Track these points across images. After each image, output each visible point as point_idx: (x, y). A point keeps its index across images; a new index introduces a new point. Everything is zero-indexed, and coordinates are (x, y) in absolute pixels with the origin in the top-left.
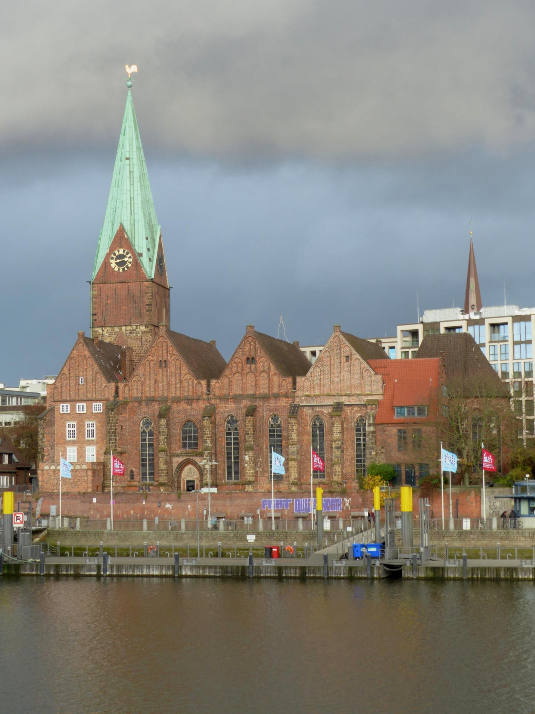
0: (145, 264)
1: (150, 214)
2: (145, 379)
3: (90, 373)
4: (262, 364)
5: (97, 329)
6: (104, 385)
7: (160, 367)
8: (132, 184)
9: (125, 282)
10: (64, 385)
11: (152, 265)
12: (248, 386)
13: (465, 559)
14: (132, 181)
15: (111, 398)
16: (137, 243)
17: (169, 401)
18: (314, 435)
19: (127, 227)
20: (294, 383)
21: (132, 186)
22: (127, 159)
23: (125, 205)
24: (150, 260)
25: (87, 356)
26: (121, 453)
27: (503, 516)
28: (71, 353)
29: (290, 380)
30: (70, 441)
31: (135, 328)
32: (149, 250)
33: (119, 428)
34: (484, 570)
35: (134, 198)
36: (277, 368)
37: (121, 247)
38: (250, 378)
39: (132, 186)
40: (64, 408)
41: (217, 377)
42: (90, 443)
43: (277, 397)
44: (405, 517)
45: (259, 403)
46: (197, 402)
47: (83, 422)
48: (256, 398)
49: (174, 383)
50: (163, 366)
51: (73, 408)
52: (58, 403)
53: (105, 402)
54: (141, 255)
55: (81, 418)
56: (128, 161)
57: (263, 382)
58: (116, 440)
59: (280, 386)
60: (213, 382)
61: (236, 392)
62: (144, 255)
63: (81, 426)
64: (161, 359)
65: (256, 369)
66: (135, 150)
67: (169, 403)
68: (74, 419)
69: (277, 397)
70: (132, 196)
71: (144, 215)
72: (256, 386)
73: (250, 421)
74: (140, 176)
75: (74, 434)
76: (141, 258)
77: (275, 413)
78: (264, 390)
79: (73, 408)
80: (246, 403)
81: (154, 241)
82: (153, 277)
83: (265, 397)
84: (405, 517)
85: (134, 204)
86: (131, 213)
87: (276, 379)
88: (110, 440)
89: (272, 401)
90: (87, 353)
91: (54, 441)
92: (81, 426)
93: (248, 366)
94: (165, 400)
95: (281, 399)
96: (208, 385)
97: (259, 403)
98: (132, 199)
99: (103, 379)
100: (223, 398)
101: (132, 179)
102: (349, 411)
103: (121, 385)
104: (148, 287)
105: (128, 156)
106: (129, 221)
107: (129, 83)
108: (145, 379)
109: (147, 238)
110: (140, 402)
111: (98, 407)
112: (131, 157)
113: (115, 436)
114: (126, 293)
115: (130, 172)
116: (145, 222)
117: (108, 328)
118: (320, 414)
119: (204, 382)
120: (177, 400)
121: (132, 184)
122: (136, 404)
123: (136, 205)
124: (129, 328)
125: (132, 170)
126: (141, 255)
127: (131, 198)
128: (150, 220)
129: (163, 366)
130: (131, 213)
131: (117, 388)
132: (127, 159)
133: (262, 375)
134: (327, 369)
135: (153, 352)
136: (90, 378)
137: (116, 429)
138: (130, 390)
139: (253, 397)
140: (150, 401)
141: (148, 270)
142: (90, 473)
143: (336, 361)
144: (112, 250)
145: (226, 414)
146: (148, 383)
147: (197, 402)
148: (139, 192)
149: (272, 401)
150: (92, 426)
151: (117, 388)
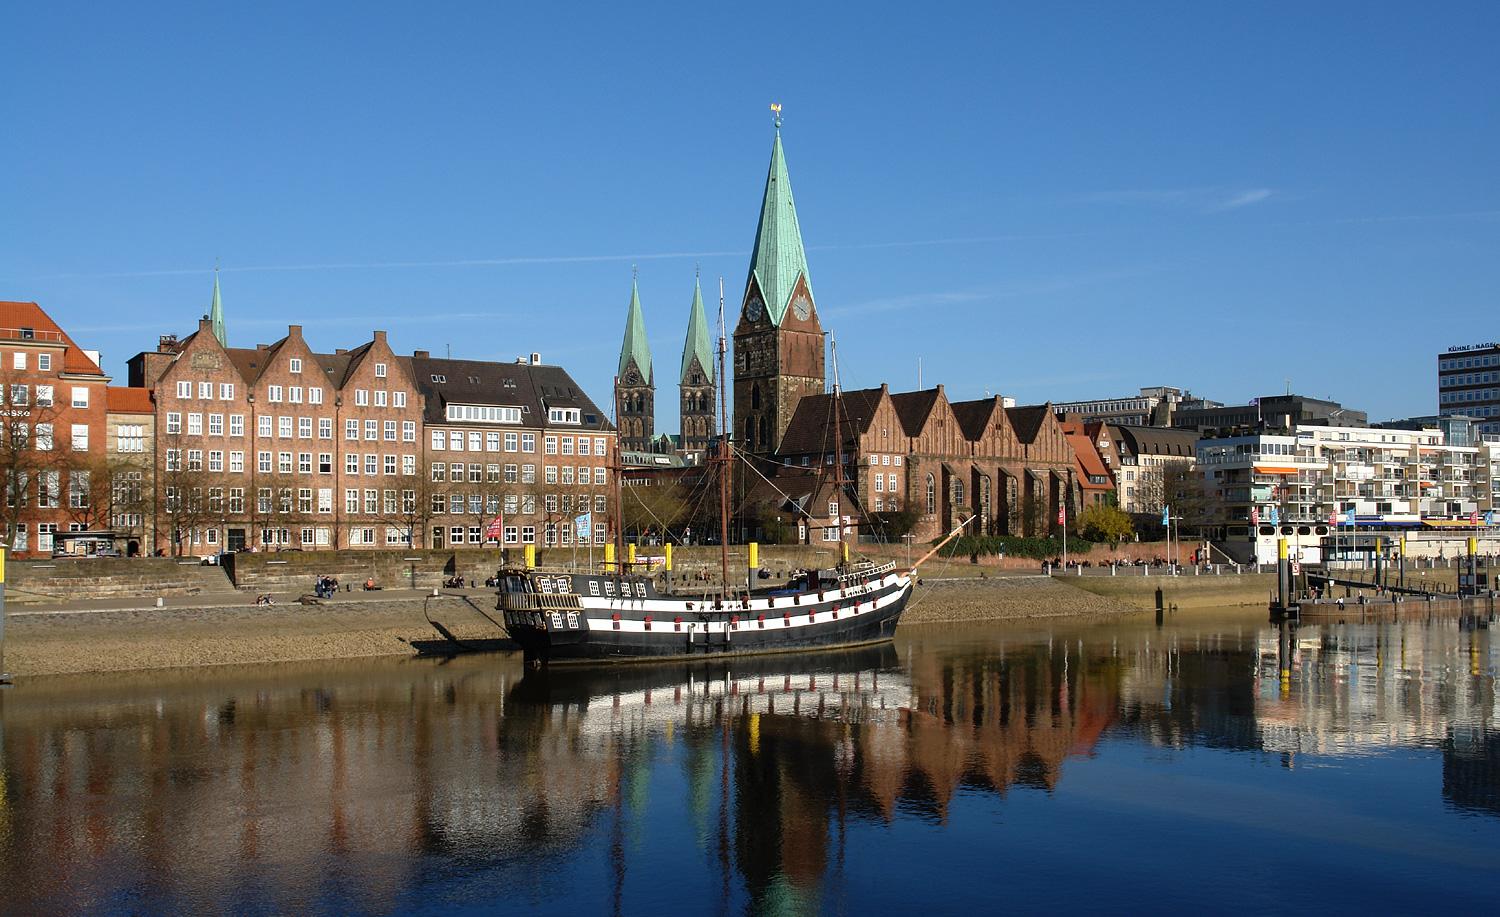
15: (908, 451)
43: (1015, 460)
51: (880, 460)
55: (886, 470)
59: (1017, 451)
60: (976, 444)
79: (880, 460)
80: (997, 465)
94: (942, 457)
111: (899, 461)
124: (808, 379)
134: (1043, 440)
138: (919, 443)
140: (934, 457)
143: (1048, 431)
144: (795, 297)
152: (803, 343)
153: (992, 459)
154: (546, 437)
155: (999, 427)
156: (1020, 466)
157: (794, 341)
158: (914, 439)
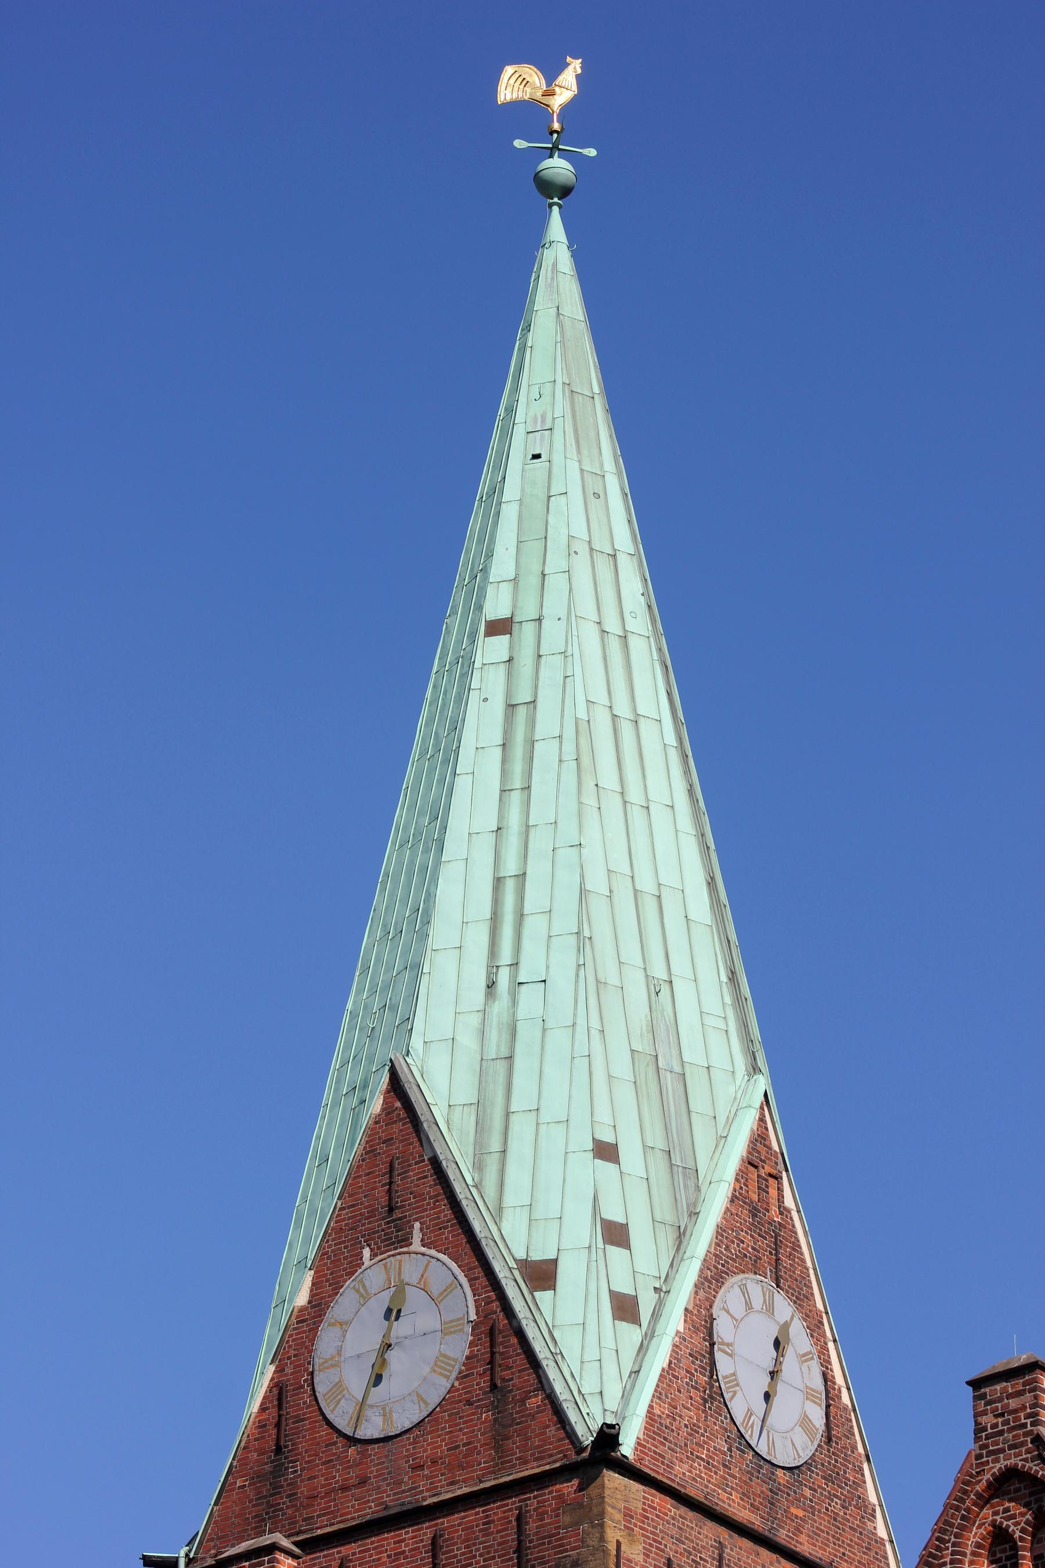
0: (569, 1341)
8: (516, 785)
11: (642, 1349)
14: (518, 767)
16: (516, 1193)
21: (516, 797)
22: (499, 627)
35: (522, 877)
39: (516, 797)
54: (542, 1275)
56: (501, 642)
70: (511, 867)
76: (544, 1297)
85: (520, 917)
86: (491, 985)
98: (510, 886)
105: (497, 607)
106: (468, 1041)
107: (558, 167)
112: (528, 610)
115: (511, 707)
121: (516, 785)
123: (534, 926)
125: (523, 695)
126: (542, 1275)
127: (498, 882)
128: (662, 1028)
130: (491, 985)
132: (499, 627)
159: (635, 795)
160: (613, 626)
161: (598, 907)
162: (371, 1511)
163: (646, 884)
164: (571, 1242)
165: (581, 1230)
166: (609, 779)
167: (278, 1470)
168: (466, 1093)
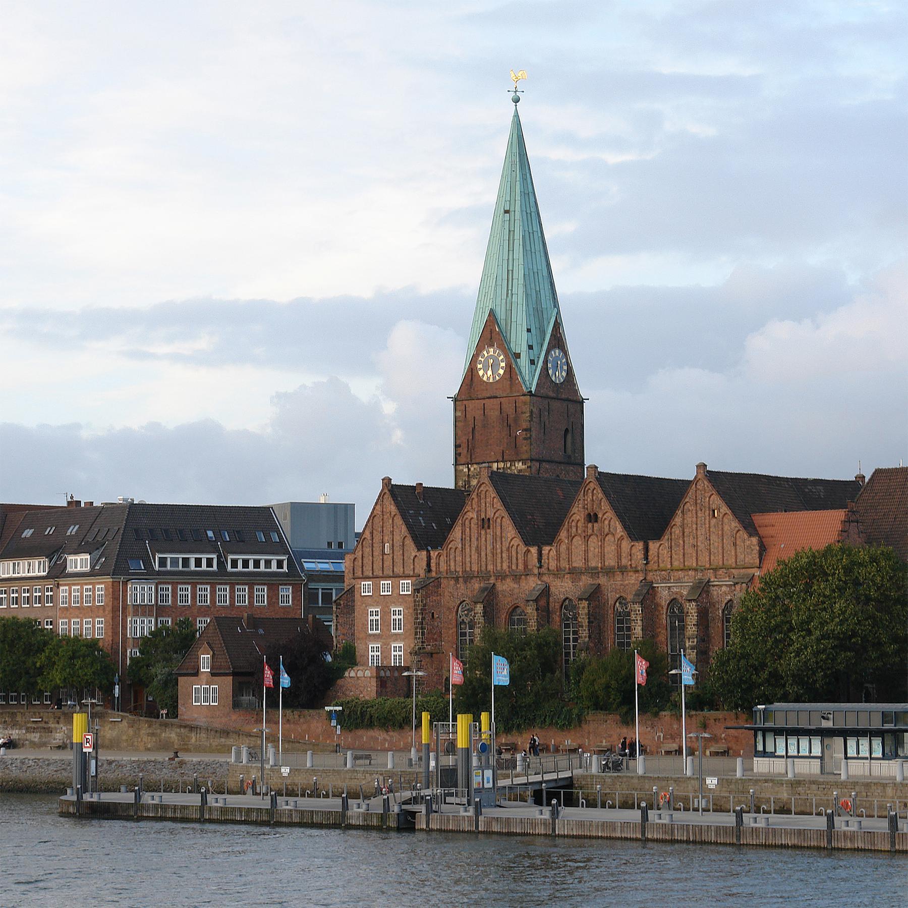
1: (538, 293)
2: (463, 545)
3: (398, 538)
4: (607, 522)
5: (461, 467)
6: (414, 554)
7: (483, 527)
9: (497, 397)
10: (366, 555)
12: (590, 554)
13: (739, 815)
15: (422, 573)
16: (513, 339)
17: (493, 578)
18: (673, 628)
19: (501, 315)
20: (646, 550)
22: (506, 212)
23: (499, 283)
24: (532, 362)
25: (393, 514)
26: (431, 654)
27: (657, 752)
28: (374, 508)
29: (640, 545)
30: (371, 635)
31: (509, 465)
32: (530, 347)
33: (428, 617)
34: (612, 825)
36: (625, 527)
37: (492, 346)
38: (594, 542)
40: (365, 588)
41: (658, 536)
42: (396, 637)
43: (623, 570)
44: (460, 753)
45: (602, 580)
46: (526, 579)
47: (388, 607)
48: (598, 573)
49: (499, 551)
50: (486, 526)
51: (376, 588)
52: (359, 581)
53: (414, 579)
54: (518, 356)
55: (385, 602)
57: (610, 549)
58: (423, 634)
61: (575, 565)
62: (523, 356)
63: (386, 614)
64: (483, 516)
65: (601, 530)
66: (518, 198)
67: (492, 581)
68: (377, 604)
69: (623, 570)
71: (527, 295)
72: (602, 556)
73: (584, 608)
74: (524, 237)
75: (377, 625)
77: (622, 595)
78: (611, 562)
79: (376, 588)
80: (586, 581)
81: (543, 333)
82: (533, 390)
83: (609, 572)
84: (460, 753)
87: (626, 544)
88: (416, 634)
89: (619, 577)
90: (393, 509)
91: (353, 634)
92: (386, 614)
93: (590, 525)
94: (484, 576)
95: (630, 574)
96: (646, 550)
97: (602, 580)
99: (413, 546)
100: (558, 573)
101: (511, 242)
102: (715, 593)
103: (434, 554)
104: (525, 403)
108: (463, 545)
109: (529, 330)
110: (457, 579)
111: (406, 586)
113: (422, 628)
114: (497, 413)
116: (527, 305)
117: (475, 466)
118: (678, 597)
119: (640, 545)
120: (502, 576)
122: (452, 582)
126: (518, 356)
128: (538, 301)
129: (486, 526)
131: (429, 558)
132: (506, 212)
133: (607, 539)
135: (474, 506)
136: (398, 544)
137: (423, 619)
138: (446, 560)
139: (594, 572)
140: (468, 578)
141: (527, 378)
142: (374, 682)
144: (479, 349)
145: (562, 597)
146: (468, 550)
147: (526, 579)
148: (521, 261)
149: (619, 577)
150: (399, 613)
151: (429, 558)
152: (494, 414)
153: (574, 572)
154: (61, 588)
155: (592, 518)
156: (633, 581)
157: (478, 414)
158: (434, 554)
159: (533, 250)
160: (529, 211)
161: (527, 278)
162: (488, 395)
163: (535, 270)
164: (523, 349)
165: (525, 347)
166: (528, 248)
167: (471, 385)
168: (503, 317)
